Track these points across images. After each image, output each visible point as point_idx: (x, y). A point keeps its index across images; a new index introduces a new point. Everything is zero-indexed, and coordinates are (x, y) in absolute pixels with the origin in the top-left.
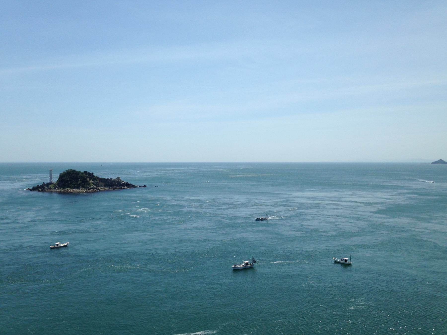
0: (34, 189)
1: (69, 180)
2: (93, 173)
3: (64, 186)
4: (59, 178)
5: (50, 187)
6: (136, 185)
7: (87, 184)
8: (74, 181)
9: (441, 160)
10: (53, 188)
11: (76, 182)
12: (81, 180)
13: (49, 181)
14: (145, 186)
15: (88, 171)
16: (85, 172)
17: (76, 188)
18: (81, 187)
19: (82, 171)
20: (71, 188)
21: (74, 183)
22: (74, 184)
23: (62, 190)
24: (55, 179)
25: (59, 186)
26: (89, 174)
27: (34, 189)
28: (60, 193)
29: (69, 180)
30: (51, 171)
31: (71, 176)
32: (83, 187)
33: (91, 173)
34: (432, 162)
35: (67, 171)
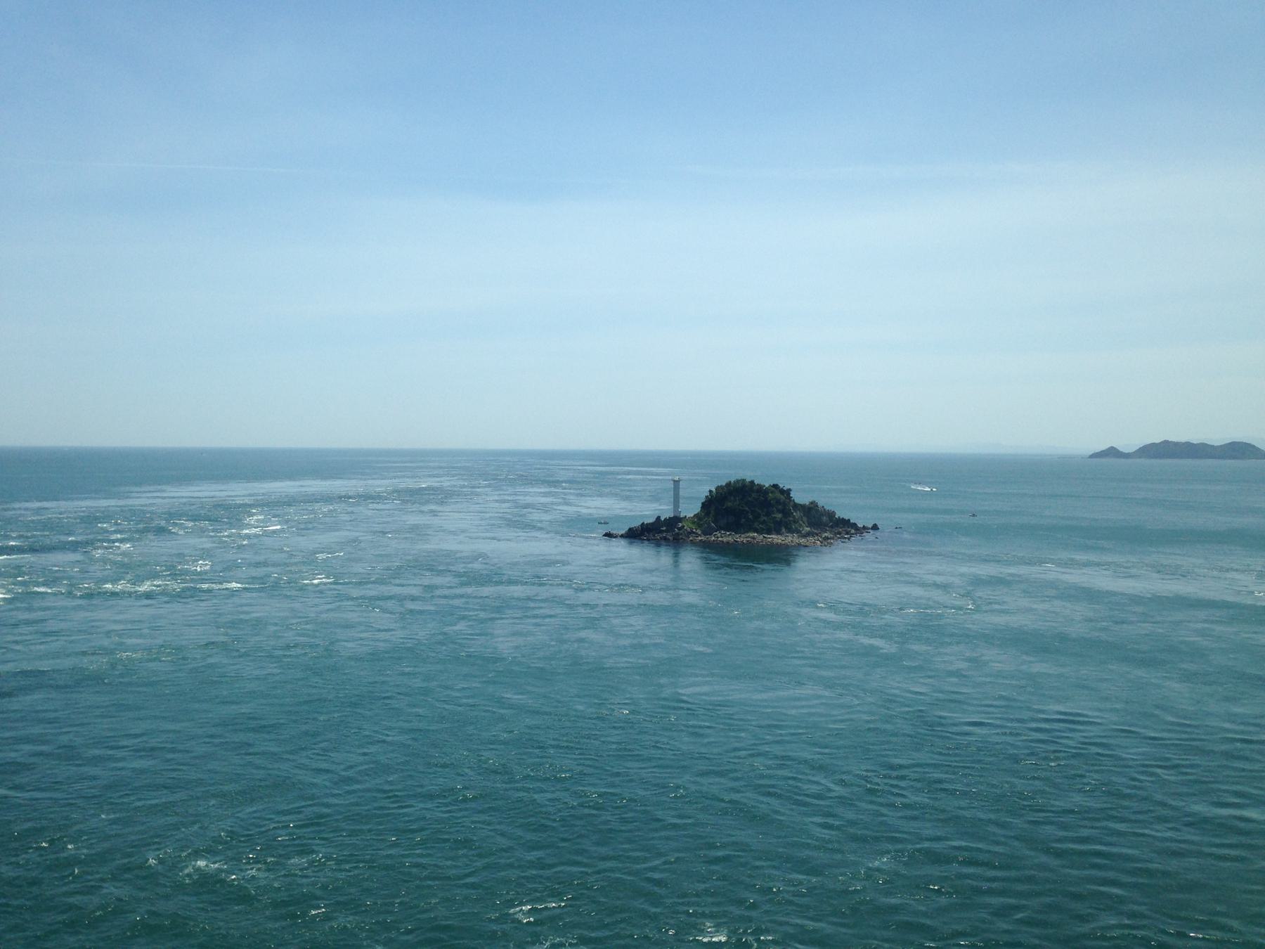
0: (640, 534)
2: (790, 490)
3: (736, 527)
4: (707, 505)
5: (689, 530)
6: (860, 525)
7: (794, 522)
8: (760, 511)
9: (1112, 448)
10: (699, 532)
11: (768, 514)
12: (779, 511)
14: (875, 527)
15: (781, 486)
16: (775, 486)
18: (784, 530)
20: (756, 531)
23: (727, 537)
24: (690, 509)
25: (720, 528)
26: (782, 491)
27: (640, 534)
28: (706, 546)
32: (790, 530)
33: (785, 489)
34: (1091, 453)
35: (729, 484)
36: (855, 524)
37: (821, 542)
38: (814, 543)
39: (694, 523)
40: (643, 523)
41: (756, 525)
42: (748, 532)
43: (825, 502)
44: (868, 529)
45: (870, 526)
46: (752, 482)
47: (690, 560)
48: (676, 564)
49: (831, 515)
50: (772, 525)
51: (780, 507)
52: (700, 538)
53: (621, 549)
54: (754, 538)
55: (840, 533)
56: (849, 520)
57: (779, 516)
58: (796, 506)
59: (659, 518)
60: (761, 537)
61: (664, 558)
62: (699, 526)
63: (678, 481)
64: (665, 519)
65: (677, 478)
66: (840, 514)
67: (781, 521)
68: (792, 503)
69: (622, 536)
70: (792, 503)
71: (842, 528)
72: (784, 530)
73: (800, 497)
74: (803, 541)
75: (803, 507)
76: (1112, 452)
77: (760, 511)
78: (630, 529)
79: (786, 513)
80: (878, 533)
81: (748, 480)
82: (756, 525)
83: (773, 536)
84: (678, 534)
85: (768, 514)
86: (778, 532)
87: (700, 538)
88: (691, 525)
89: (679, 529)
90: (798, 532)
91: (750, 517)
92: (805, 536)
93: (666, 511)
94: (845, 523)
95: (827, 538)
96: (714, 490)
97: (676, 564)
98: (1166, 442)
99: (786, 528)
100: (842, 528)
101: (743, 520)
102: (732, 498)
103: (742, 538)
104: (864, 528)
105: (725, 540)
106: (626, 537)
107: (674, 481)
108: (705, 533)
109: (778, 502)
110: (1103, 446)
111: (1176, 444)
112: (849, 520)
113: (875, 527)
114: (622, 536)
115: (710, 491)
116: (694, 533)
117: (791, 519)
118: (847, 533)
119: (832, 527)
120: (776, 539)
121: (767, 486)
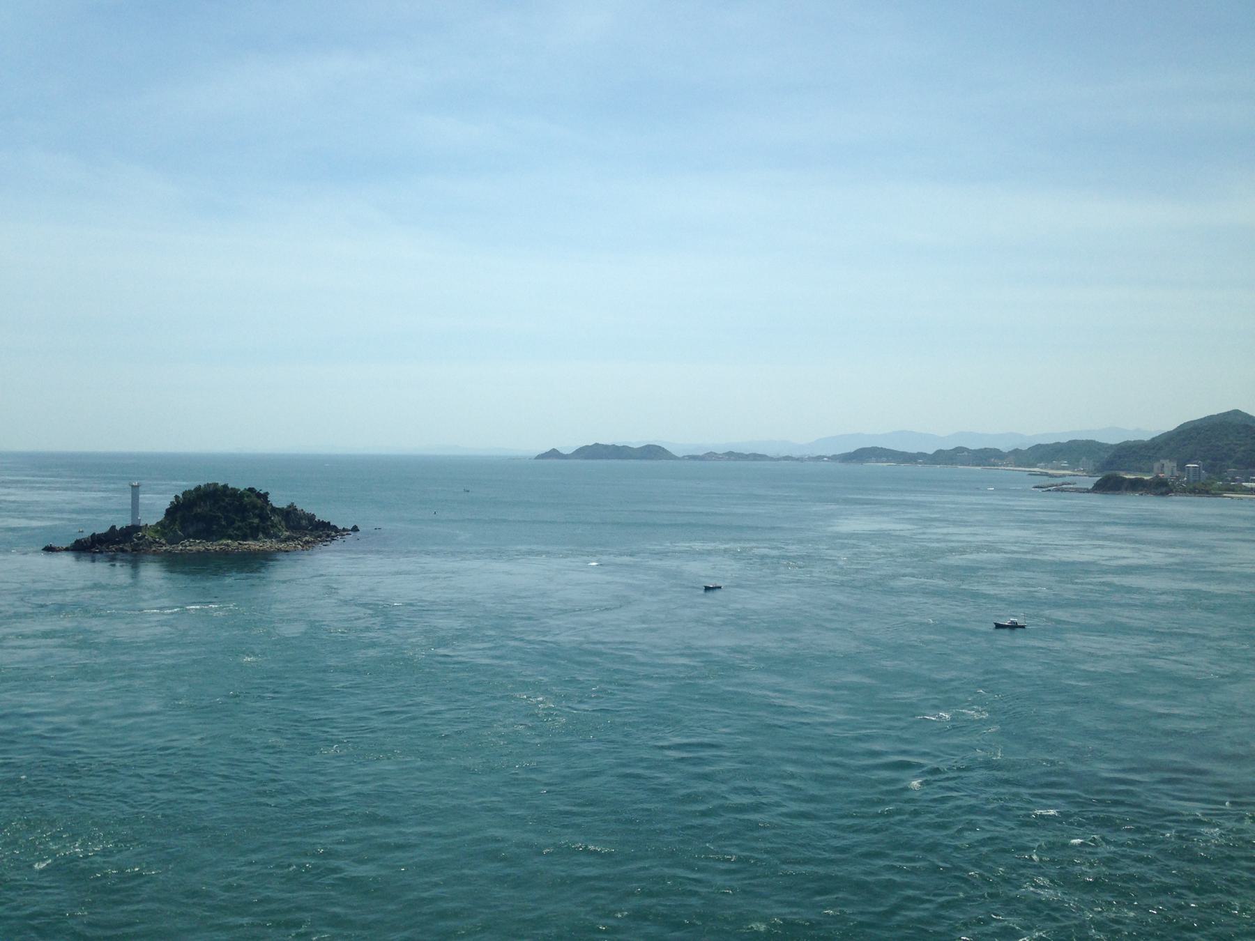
0: (87, 547)
1: (220, 514)
2: (267, 493)
3: (207, 535)
4: (169, 512)
6: (340, 527)
7: (272, 526)
8: (234, 516)
11: (243, 520)
13: (130, 524)
14: (355, 529)
16: (251, 490)
17: (250, 538)
18: (261, 535)
19: (242, 486)
20: (230, 537)
21: (238, 524)
22: (239, 528)
23: (197, 546)
25: (188, 537)
26: (259, 495)
29: (220, 514)
30: (135, 490)
31: (223, 504)
32: (268, 536)
33: (262, 492)
35: (198, 489)
36: (335, 526)
37: (303, 547)
38: (295, 547)
39: (157, 532)
40: (94, 534)
41: (230, 532)
42: (220, 539)
43: (305, 507)
44: (349, 530)
45: (350, 528)
46: (225, 486)
47: (152, 573)
48: (135, 576)
49: (311, 518)
50: (248, 531)
51: (257, 511)
52: (164, 548)
53: (65, 561)
54: (228, 545)
55: (320, 536)
56: (329, 523)
57: (256, 521)
58: (274, 510)
59: (113, 527)
60: (236, 543)
61: (120, 574)
62: (164, 535)
63: (138, 486)
64: (122, 529)
65: (135, 483)
66: (321, 516)
67: (258, 526)
68: (269, 508)
69: (67, 549)
70: (269, 508)
71: (323, 531)
72: (261, 535)
73: (279, 500)
74: (283, 545)
75: (281, 510)
76: (554, 454)
77: (234, 516)
78: (77, 541)
79: (263, 517)
80: (358, 534)
81: (221, 483)
82: (230, 532)
83: (250, 543)
84: (137, 544)
85: (243, 519)
86: (255, 538)
87: (164, 548)
88: (153, 534)
89: (139, 539)
90: (277, 537)
91: (223, 523)
92: (285, 541)
93: (122, 522)
94: (325, 526)
95: (308, 542)
96: (181, 496)
97: (135, 576)
98: (597, 444)
99: (263, 533)
100: (323, 531)
101: (215, 527)
102: (202, 503)
103: (213, 546)
104: (344, 530)
105: (194, 548)
106: (72, 550)
107: (133, 486)
108: (170, 542)
109: (255, 507)
110: (547, 449)
111: (606, 447)
112: (329, 523)
113: (355, 529)
114: (67, 549)
115: (176, 497)
116: (157, 542)
117: (269, 523)
118: (328, 536)
119: (311, 530)
120: (253, 545)
121: (242, 489)
